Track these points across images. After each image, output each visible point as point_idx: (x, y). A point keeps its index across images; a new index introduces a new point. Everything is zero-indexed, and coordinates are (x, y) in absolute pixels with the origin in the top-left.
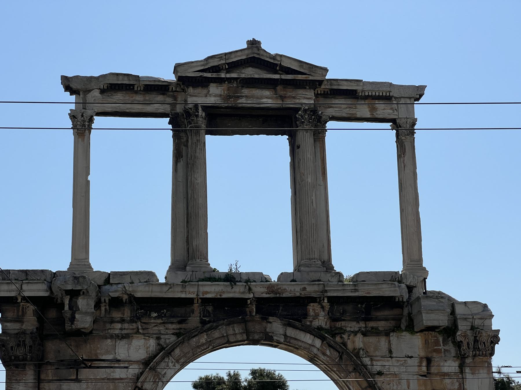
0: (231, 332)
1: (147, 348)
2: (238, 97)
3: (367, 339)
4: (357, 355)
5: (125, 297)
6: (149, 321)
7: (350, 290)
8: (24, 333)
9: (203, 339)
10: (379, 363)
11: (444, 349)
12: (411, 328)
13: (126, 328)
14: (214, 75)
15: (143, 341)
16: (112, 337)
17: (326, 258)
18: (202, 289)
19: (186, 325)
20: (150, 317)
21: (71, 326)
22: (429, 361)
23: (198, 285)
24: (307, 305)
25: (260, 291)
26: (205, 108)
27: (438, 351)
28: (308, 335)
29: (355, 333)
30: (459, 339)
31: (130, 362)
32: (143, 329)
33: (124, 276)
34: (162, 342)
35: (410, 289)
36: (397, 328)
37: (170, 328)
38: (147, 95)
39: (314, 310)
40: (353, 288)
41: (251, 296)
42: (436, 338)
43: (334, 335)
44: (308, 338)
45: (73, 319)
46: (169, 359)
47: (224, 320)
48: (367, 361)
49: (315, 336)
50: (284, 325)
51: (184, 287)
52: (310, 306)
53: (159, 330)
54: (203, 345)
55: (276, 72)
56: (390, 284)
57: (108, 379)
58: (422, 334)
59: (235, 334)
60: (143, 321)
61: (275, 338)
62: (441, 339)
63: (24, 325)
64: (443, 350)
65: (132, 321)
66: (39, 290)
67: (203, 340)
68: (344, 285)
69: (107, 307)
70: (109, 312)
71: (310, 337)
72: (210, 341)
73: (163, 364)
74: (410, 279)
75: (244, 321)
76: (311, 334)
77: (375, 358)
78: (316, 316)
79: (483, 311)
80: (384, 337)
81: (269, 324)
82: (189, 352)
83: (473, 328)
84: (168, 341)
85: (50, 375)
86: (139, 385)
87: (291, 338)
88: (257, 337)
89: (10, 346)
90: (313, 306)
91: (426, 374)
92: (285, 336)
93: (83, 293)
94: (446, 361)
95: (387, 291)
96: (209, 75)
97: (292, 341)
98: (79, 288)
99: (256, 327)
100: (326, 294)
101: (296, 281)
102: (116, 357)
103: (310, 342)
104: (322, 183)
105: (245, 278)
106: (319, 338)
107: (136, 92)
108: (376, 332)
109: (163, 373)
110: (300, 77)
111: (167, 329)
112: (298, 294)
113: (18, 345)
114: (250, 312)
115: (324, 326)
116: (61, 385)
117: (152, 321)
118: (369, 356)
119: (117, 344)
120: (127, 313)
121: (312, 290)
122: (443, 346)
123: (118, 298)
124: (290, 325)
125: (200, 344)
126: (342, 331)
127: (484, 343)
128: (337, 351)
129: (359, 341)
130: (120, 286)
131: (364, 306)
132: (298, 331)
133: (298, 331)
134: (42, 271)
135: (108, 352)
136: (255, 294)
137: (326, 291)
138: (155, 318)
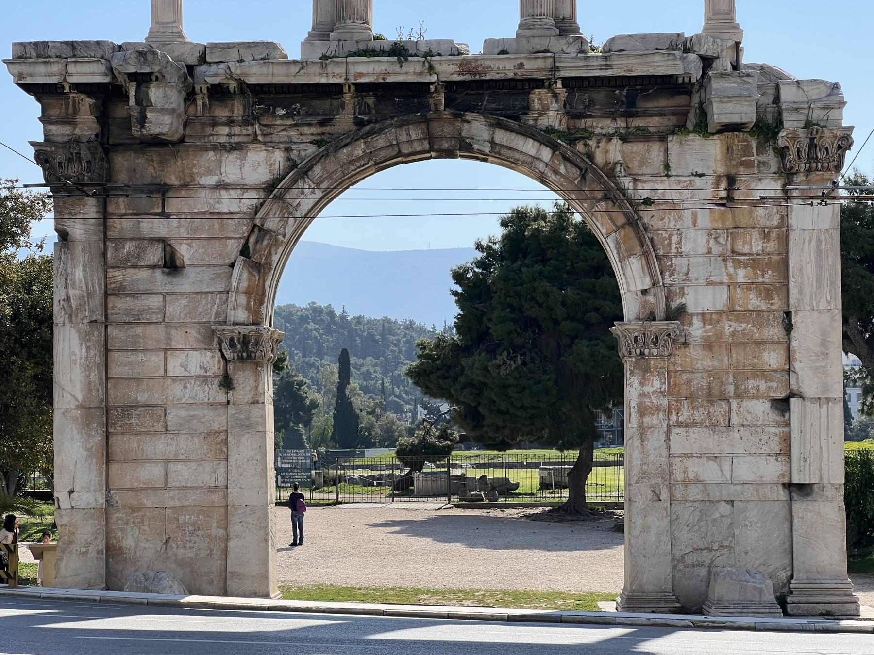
0: (404, 138)
1: (271, 165)
3: (628, 147)
4: (611, 173)
5: (233, 85)
6: (273, 123)
7: (597, 66)
8: (77, 141)
9: (359, 149)
10: (647, 186)
11: (759, 161)
12: (703, 128)
13: (237, 133)
15: (264, 154)
16: (215, 148)
17: (567, 13)
18: (353, 69)
19: (332, 128)
20: (274, 115)
21: (141, 131)
22: (731, 180)
23: (347, 62)
24: (529, 93)
25: (448, 70)
27: (748, 165)
28: (531, 141)
29: (609, 137)
30: (781, 143)
31: (245, 188)
32: (264, 135)
33: (228, 50)
34: (294, 155)
35: (707, 62)
36: (680, 128)
37: (306, 132)
39: (540, 100)
40: (604, 63)
41: (434, 78)
42: (745, 143)
43: (572, 142)
44: (529, 147)
45: (142, 120)
46: (305, 182)
47: (392, 118)
48: (627, 182)
49: (541, 143)
51: (324, 66)
52: (534, 93)
53: (290, 137)
54: (359, 159)
56: (666, 55)
57: (211, 213)
58: (723, 137)
59: (410, 142)
60: (263, 122)
61: (476, 146)
62: (754, 144)
63: (77, 129)
64: (756, 162)
65: (245, 123)
66: (93, 74)
67: (359, 152)
68: (586, 58)
69: (207, 101)
70: (210, 108)
71: (533, 144)
72: (371, 153)
73: (294, 192)
74: (706, 45)
75: (427, 121)
76: (534, 140)
77: (641, 178)
78: (545, 110)
79: (830, 95)
80: (658, 143)
81: (465, 124)
82: (336, 171)
83: (808, 124)
84: (303, 154)
86: (258, 222)
87: (502, 146)
88: (445, 145)
89: (57, 161)
90: (540, 93)
91: (725, 201)
92: (492, 142)
93: (157, 78)
94: (760, 180)
95: (660, 66)
98: (147, 70)
99: (445, 129)
100: (557, 74)
101: (508, 54)
102: (223, 179)
103: (533, 152)
105: (423, 49)
106: (547, 146)
108: (644, 135)
109: (295, 204)
111: (301, 134)
112: (511, 75)
113: (70, 160)
114: (436, 105)
115: (557, 126)
116: (139, 222)
117: (278, 122)
118: (630, 174)
119: (223, 158)
120: (238, 110)
121: (534, 67)
122: (758, 155)
123: (219, 85)
124: (500, 125)
125: (353, 158)
126: (586, 135)
127: (827, 148)
128: (577, 166)
129: (614, 151)
130: (222, 66)
131: (625, 92)
132: (513, 136)
133: (514, 134)
134: (98, 43)
135: (209, 172)
136: (440, 76)
137: (558, 69)
138: (283, 117)
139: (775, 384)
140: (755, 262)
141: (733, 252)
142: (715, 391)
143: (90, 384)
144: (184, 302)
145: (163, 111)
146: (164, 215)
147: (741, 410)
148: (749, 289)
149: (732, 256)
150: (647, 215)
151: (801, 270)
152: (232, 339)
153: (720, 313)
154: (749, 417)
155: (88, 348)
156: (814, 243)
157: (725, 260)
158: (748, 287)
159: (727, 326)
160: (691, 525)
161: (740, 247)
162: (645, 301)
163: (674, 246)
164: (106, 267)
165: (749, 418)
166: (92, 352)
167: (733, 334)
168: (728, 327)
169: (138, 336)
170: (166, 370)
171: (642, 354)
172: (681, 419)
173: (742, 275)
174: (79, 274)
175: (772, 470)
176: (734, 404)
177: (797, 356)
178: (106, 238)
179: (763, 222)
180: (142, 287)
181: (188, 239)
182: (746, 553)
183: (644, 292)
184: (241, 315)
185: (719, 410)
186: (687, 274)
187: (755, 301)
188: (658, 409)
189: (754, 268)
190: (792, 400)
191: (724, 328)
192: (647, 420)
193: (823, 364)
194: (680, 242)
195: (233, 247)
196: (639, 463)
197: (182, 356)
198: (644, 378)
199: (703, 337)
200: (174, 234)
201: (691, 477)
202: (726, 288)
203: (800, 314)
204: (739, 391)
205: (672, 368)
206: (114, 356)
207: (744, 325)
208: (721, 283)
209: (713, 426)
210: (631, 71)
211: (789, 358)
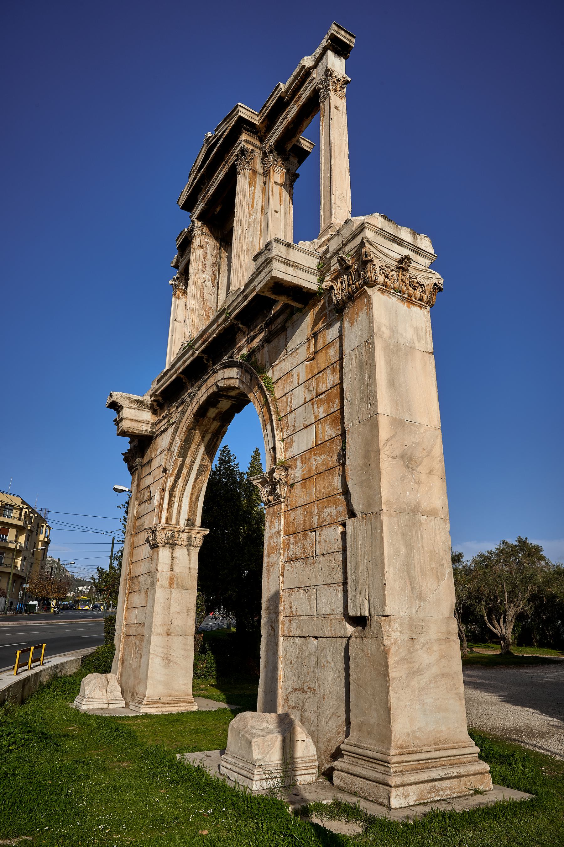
148: (325, 422)
157: (313, 404)
160: (293, 663)
163: (288, 406)
165: (326, 548)
172: (289, 556)
182: (324, 698)
185: (307, 543)
186: (294, 425)
189: (328, 403)
191: (312, 464)
192: (271, 559)
194: (291, 402)
198: (271, 522)
201: (294, 613)
204: (321, 520)
207: (322, 457)
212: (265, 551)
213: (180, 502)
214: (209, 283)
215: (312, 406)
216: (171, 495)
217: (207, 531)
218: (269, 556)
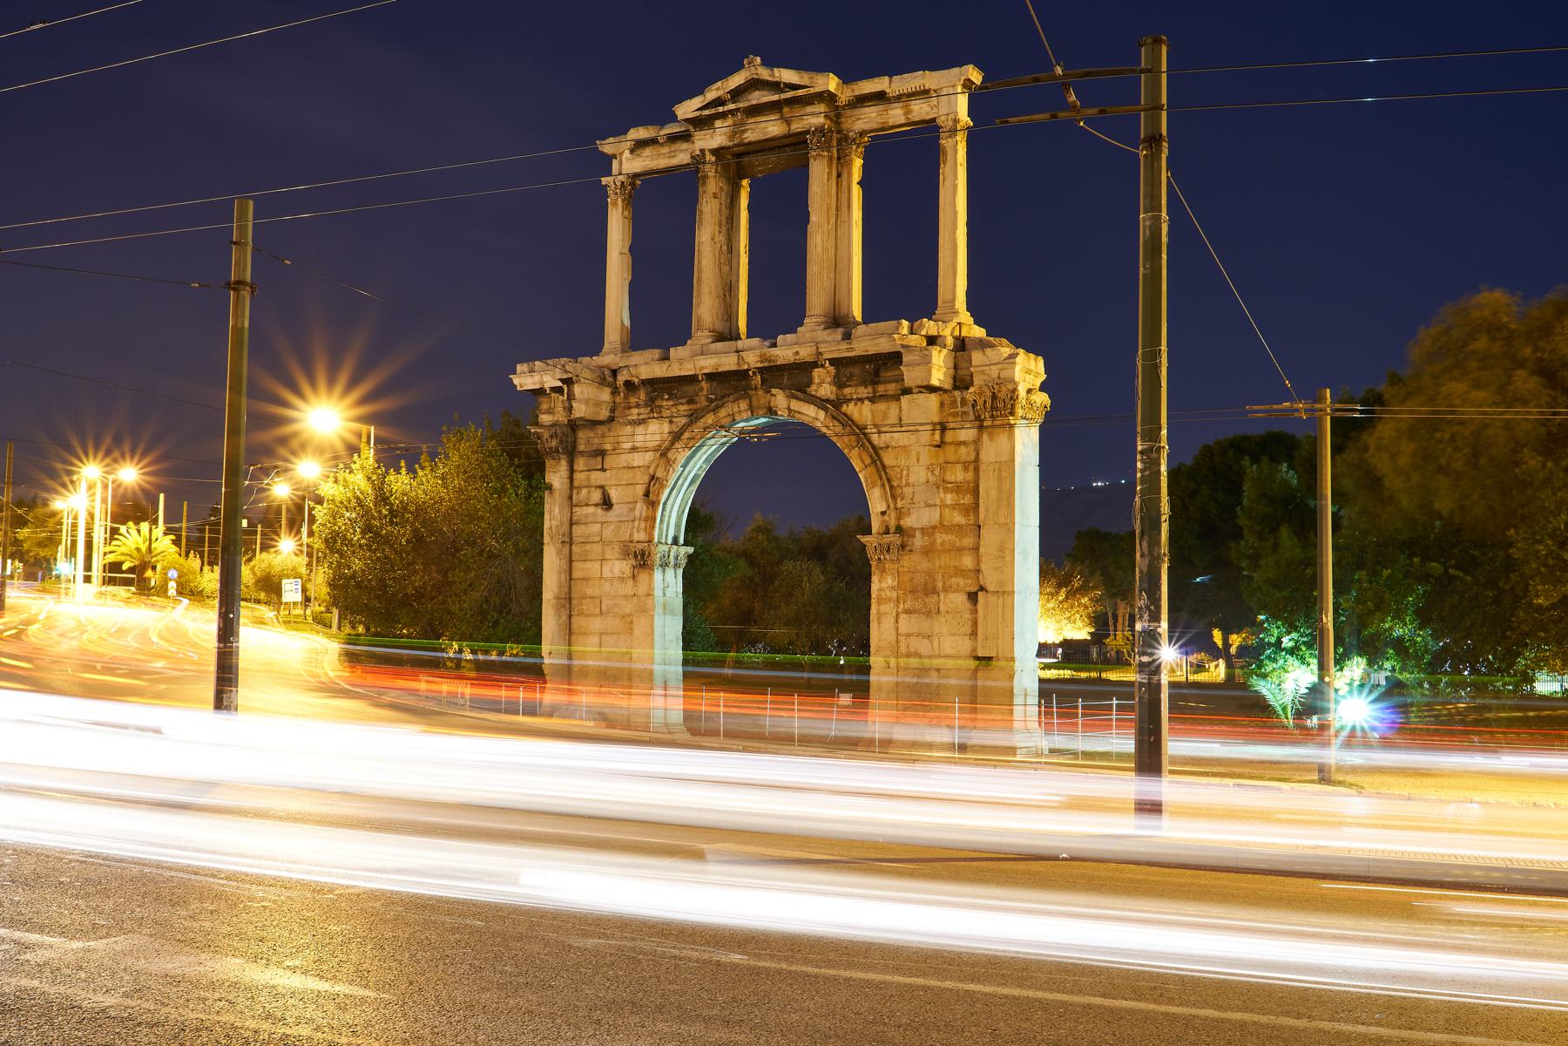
2: (744, 131)
14: (713, 111)
20: (663, 399)
26: (714, 152)
29: (861, 400)
38: (672, 145)
39: (819, 376)
50: (788, 397)
55: (782, 91)
57: (629, 468)
60: (657, 404)
76: (815, 405)
85: (581, 466)
87: (795, 411)
92: (789, 409)
96: (706, 112)
97: (796, 415)
104: (847, 220)
107: (662, 145)
110: (800, 92)
117: (665, 403)
124: (794, 397)
139: (970, 581)
140: (958, 489)
141: (944, 481)
142: (930, 586)
143: (560, 583)
144: (612, 527)
145: (580, 401)
146: (603, 470)
147: (947, 600)
148: (954, 509)
149: (941, 484)
150: (888, 459)
151: (987, 493)
152: (635, 552)
153: (934, 528)
154: (952, 606)
155: (560, 559)
156: (996, 473)
157: (938, 488)
158: (954, 507)
159: (938, 537)
161: (950, 477)
162: (884, 521)
163: (904, 478)
164: (572, 506)
166: (562, 562)
167: (942, 544)
168: (940, 538)
169: (587, 551)
170: (601, 574)
171: (879, 559)
173: (949, 499)
174: (557, 510)
175: (965, 645)
176: (942, 595)
177: (984, 559)
178: (571, 487)
179: (964, 458)
180: (590, 519)
181: (616, 485)
183: (883, 513)
184: (642, 536)
185: (932, 600)
186: (912, 499)
187: (958, 518)
188: (890, 600)
189: (957, 493)
190: (980, 594)
191: (936, 538)
192: (883, 608)
193: (1001, 565)
194: (908, 475)
195: (640, 490)
196: (876, 639)
197: (610, 563)
199: (922, 546)
200: (608, 483)
202: (939, 508)
203: (986, 527)
205: (901, 569)
206: (576, 565)
207: (950, 536)
208: (935, 505)
209: (928, 614)
210: (867, 351)
211: (978, 562)
212: (873, 601)
213: (670, 517)
214: (725, 248)
215: (936, 490)
216: (664, 509)
217: (691, 550)
218: (879, 603)
